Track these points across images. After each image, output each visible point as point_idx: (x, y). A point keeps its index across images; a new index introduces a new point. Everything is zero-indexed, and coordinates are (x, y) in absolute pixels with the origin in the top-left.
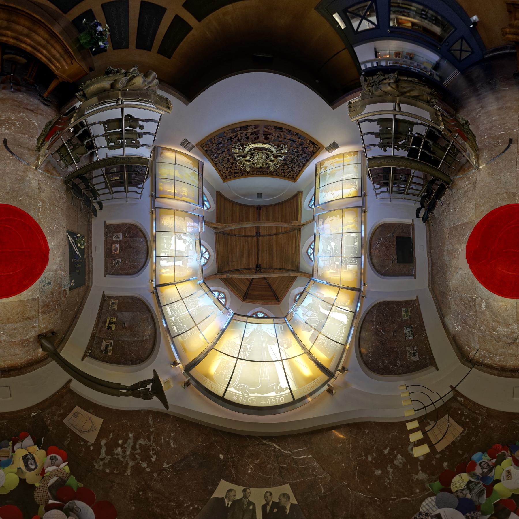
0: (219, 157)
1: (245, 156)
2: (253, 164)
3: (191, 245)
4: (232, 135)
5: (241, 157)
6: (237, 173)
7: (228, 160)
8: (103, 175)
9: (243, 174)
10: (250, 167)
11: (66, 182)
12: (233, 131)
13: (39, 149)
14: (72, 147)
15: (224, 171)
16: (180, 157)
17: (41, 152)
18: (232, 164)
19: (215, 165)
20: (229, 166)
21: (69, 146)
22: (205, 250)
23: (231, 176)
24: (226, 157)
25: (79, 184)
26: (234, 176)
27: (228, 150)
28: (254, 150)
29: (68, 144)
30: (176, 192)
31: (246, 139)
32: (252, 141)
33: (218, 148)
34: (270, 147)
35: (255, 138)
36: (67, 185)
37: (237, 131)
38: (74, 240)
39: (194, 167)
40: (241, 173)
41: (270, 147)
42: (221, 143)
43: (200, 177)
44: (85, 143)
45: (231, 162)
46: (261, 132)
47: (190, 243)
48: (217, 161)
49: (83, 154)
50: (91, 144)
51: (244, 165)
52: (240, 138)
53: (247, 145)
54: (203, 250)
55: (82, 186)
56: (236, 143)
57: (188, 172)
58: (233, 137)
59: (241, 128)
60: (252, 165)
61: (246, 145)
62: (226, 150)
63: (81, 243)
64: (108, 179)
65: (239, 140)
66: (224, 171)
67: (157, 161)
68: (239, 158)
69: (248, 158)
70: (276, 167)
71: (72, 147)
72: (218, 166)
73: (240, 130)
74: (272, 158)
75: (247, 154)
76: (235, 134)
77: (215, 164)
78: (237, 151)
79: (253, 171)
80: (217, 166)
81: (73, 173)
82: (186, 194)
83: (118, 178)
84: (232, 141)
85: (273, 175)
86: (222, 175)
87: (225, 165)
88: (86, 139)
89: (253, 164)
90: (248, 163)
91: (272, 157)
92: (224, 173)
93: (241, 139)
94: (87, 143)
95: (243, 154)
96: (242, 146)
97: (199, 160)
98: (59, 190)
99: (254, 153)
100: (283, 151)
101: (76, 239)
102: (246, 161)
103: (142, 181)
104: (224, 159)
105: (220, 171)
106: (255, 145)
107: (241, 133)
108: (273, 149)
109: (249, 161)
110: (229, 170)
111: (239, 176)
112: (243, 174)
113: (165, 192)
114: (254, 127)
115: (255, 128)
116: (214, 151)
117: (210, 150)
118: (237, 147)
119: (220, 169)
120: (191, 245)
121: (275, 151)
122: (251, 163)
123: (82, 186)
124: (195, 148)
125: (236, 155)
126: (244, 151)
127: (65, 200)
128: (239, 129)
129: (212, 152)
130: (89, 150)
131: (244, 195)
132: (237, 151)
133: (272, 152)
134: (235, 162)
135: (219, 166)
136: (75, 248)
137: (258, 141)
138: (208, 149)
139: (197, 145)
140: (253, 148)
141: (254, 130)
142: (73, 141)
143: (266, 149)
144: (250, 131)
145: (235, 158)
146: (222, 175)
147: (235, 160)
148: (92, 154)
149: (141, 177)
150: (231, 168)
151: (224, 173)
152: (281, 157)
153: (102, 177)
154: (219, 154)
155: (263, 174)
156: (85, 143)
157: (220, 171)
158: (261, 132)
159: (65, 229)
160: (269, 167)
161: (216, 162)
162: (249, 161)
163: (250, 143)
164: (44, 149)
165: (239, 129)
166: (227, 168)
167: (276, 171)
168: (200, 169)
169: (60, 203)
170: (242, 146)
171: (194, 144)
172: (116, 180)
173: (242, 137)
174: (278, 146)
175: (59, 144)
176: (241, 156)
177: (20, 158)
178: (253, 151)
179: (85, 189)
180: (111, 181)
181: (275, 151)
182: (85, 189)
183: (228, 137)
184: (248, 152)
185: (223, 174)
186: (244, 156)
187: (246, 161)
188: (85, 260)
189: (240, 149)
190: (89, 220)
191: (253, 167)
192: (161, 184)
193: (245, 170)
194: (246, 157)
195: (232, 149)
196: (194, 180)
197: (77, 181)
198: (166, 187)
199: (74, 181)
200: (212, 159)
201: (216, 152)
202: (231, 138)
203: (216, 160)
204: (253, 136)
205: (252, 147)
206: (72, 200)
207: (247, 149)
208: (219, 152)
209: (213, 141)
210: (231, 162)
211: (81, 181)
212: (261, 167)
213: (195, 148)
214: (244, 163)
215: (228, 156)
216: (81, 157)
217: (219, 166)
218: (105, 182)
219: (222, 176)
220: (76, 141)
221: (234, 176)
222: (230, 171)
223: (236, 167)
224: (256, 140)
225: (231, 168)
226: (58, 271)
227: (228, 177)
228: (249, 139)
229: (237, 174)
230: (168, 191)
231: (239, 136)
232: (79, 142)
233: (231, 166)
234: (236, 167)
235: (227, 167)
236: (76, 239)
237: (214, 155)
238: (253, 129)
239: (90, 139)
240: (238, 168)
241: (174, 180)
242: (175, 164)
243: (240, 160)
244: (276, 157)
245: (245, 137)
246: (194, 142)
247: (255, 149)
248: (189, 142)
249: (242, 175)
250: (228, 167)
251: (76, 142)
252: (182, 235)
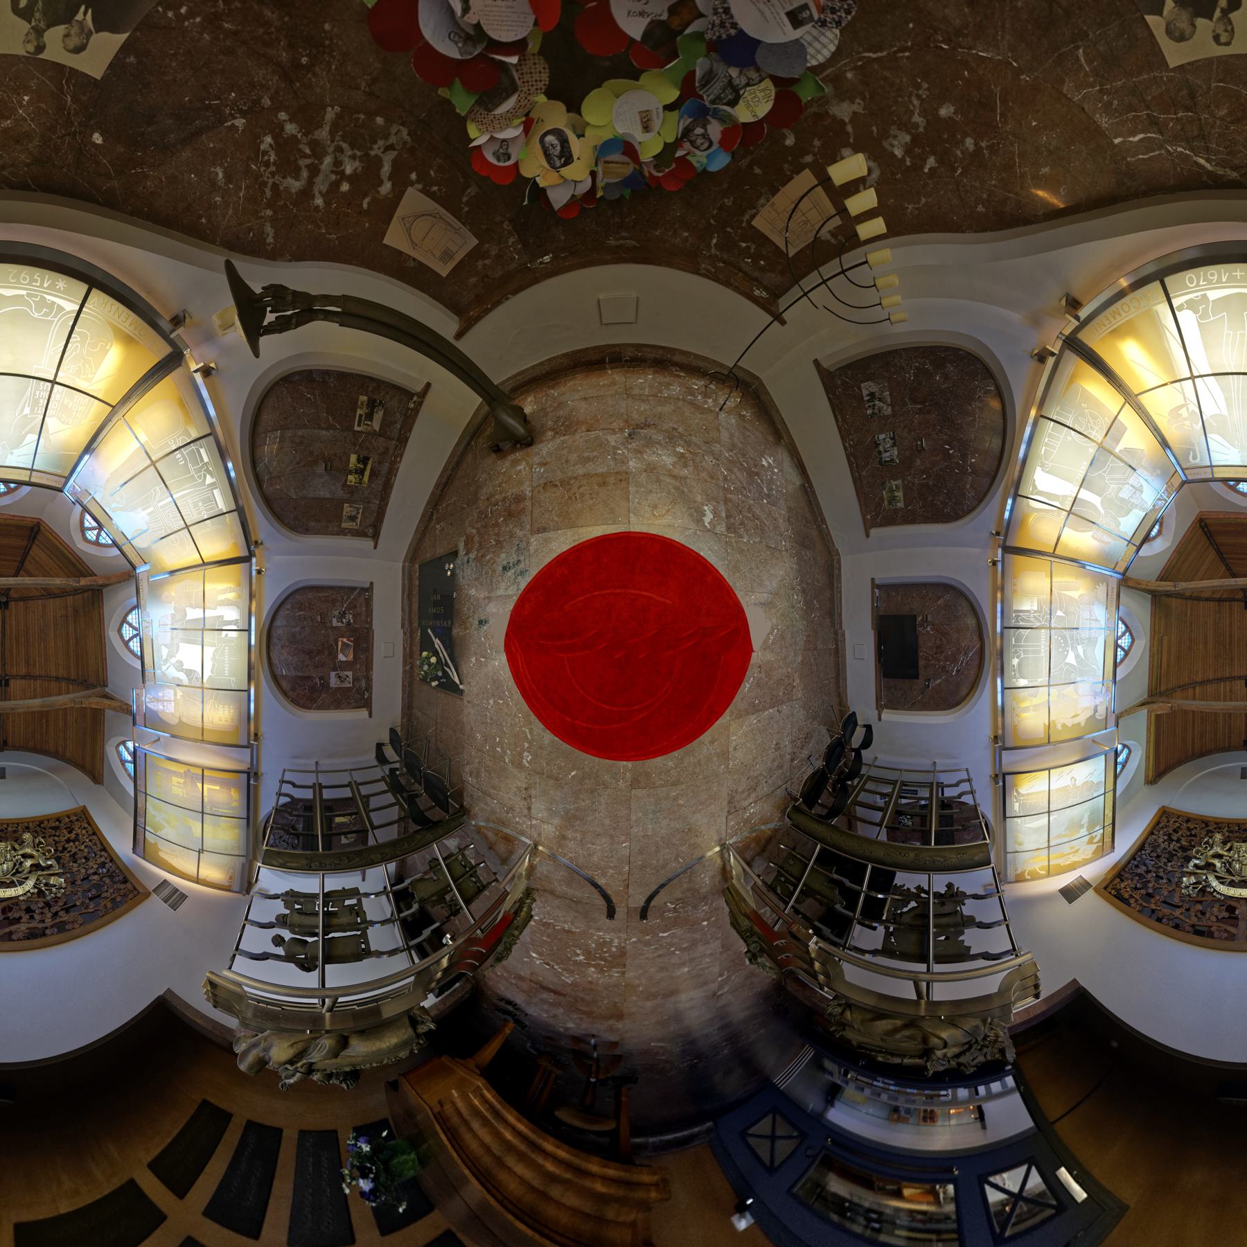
0: (96, 866)
1: (34, 868)
2: (15, 850)
3: (164, 658)
4: (64, 917)
5: (43, 864)
6: (52, 828)
7: (74, 858)
8: (374, 828)
9: (39, 826)
10: (22, 843)
11: (463, 812)
12: (61, 927)
13: (528, 893)
14: (448, 898)
15: (84, 832)
16: (189, 866)
17: (522, 885)
18: (64, 849)
19: (105, 847)
20: (71, 844)
21: (454, 900)
22: (131, 644)
23: (67, 820)
24: (79, 865)
25: (432, 808)
26: (60, 822)
27: (73, 883)
28: (13, 882)
29: (456, 903)
30: (200, 785)
31: (33, 907)
32: (17, 904)
33: (98, 886)
35: (10, 909)
36: (462, 806)
37: (52, 926)
38: (445, 672)
39: (156, 843)
40: (45, 828)
42: (91, 899)
43: (140, 820)
44: (415, 907)
45: (68, 855)
47: (166, 661)
48: (101, 856)
49: (422, 879)
50: (402, 904)
51: (36, 846)
52: (46, 910)
53: (29, 894)
54: (135, 645)
55: (424, 801)
56: (56, 899)
57: (169, 832)
58: (62, 913)
59: (44, 935)
60: (17, 846)
61: (32, 894)
62: (79, 882)
63: (430, 665)
64: (361, 817)
65: (48, 905)
66: (84, 832)
67: (243, 860)
68: (49, 863)
69: (28, 863)
71: (448, 898)
72: (99, 845)
73: (46, 928)
75: (30, 872)
76: (58, 920)
77: (104, 849)
78: (52, 881)
79: (15, 832)
80: (102, 844)
81: (446, 833)
82: (175, 779)
83: (338, 820)
84: (65, 904)
86: (89, 824)
87: (82, 847)
88: (413, 915)
89: (15, 850)
90: (28, 851)
92: (85, 828)
93: (42, 908)
94: (410, 907)
95: (40, 873)
96: (41, 893)
97: (144, 859)
98: (480, 794)
99: (14, 875)
101: (440, 674)
102: (31, 857)
103: (281, 811)
104: (84, 861)
105: (94, 834)
107: (44, 922)
109: (25, 856)
110: (73, 836)
111: (48, 820)
112: (39, 826)
113: (225, 784)
114: (14, 937)
115: (11, 933)
116: (107, 880)
117: (116, 883)
118: (54, 889)
119: (95, 837)
120: (164, 658)
122: (21, 852)
123: (424, 801)
124: (151, 888)
125: (57, 869)
126: (38, 879)
127: (467, 769)
128: (48, 932)
129: (111, 877)
130: (406, 889)
131: (37, 774)
132: (52, 881)
134: (58, 854)
135: (95, 844)
136: (444, 654)
137: (4, 904)
138: (122, 886)
139: (148, 895)
140: (16, 886)
141: (13, 928)
142: (445, 913)
144: (23, 927)
145: (58, 863)
146: (89, 824)
147: (58, 859)
148: (399, 878)
149: (281, 821)
150: (68, 841)
151: (85, 828)
153: (376, 823)
154: (95, 873)
156: (415, 907)
157: (94, 834)
159: (466, 698)
161: (103, 853)
162: (25, 856)
163: (21, 898)
164: (516, 894)
165: (48, 932)
168: (140, 837)
169: (479, 763)
170: (41, 893)
171: (154, 896)
172: (343, 815)
173: (42, 913)
175: (480, 905)
176: (43, 869)
177: (575, 874)
178: (15, 879)
179: (417, 796)
180: (356, 814)
182: (417, 796)
183: (73, 914)
184: (27, 878)
185: (86, 825)
186: (36, 867)
187: (31, 857)
188: (420, 624)
189: (46, 885)
190: (409, 720)
191: (16, 841)
192: (235, 804)
193: (35, 834)
194: (31, 865)
195: (64, 885)
196: (155, 813)
197: (436, 814)
198: (223, 796)
199: (444, 814)
200: (112, 860)
201: (101, 878)
202: (67, 910)
203: (103, 859)
204: (16, 915)
205: (19, 888)
206: (450, 767)
207: (29, 885)
208: (96, 877)
209: (109, 905)
210: (68, 855)
211: (426, 813)
213: (151, 888)
214: (38, 851)
215: (75, 869)
216: (426, 873)
217: (95, 844)
218: (368, 812)
219: (90, 822)
220: (438, 911)
221: (60, 822)
222: (70, 832)
223: (56, 843)
225: (68, 841)
226: (484, 599)
227: (75, 818)
228: (24, 907)
229: (53, 825)
230: (218, 788)
231: (49, 915)
232: (429, 908)
233: (67, 846)
234: (56, 843)
235: (77, 843)
236: (440, 674)
237: (108, 870)
238: (16, 931)
239: (402, 915)
240: (51, 839)
241: (203, 813)
242: (201, 851)
243: (47, 859)
245: (34, 912)
246: (155, 902)
247: (12, 885)
248: (166, 902)
249: (42, 822)
250: (74, 841)
251: (438, 908)
252: (185, 681)
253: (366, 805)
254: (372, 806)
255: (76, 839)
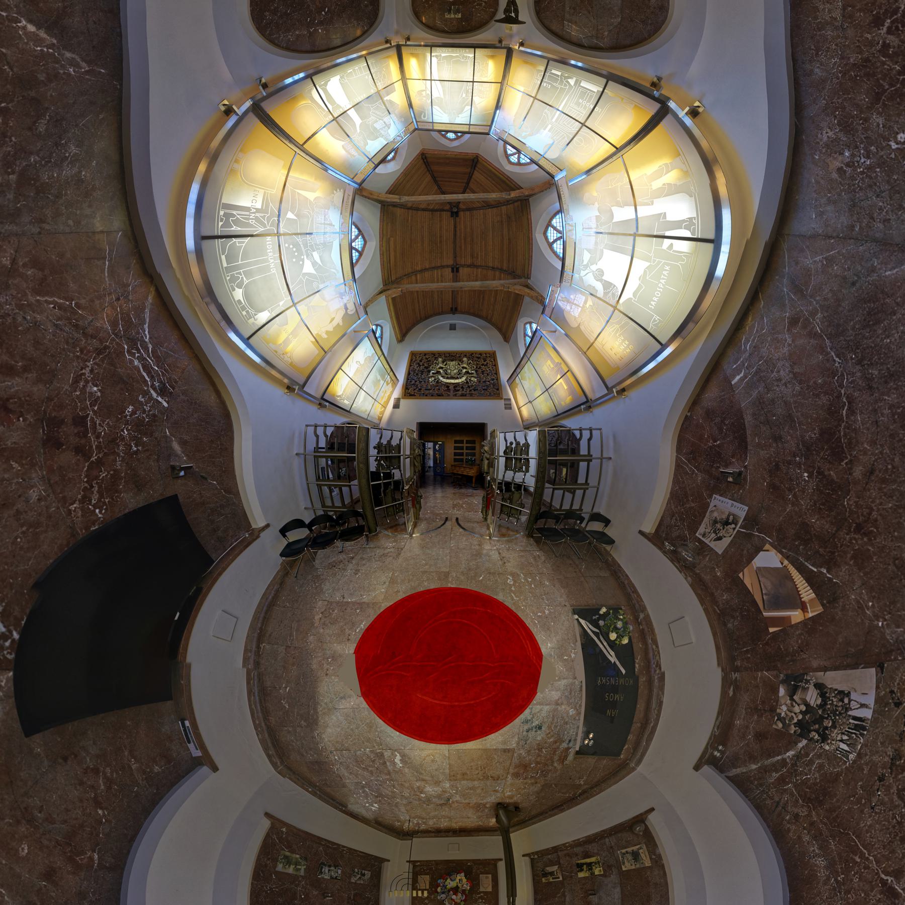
2: (459, 365)
18: (480, 368)
23: (485, 355)
34: (445, 380)
41: (445, 380)
46: (452, 392)
51: (469, 364)
56: (472, 386)
69: (464, 371)
70: (436, 363)
74: (441, 371)
83: (564, 470)
85: (438, 354)
89: (459, 365)
90: (465, 366)
91: (442, 371)
100: (433, 379)
102: (466, 368)
106: (457, 381)
108: (441, 379)
109: (463, 368)
110: (485, 363)
121: (440, 377)
125: (475, 375)
132: (472, 379)
133: (442, 376)
143: (448, 378)
144: (460, 393)
147: (476, 371)
150: (483, 365)
152: (433, 373)
155: (449, 354)
157: (495, 365)
158: (452, 392)
160: (443, 362)
166: (486, 365)
167: (436, 358)
174: (437, 382)
176: (470, 374)
180: (566, 482)
181: (440, 377)
186: (467, 373)
187: (466, 368)
207: (464, 379)
212: (452, 361)
224: (456, 385)
244: (438, 373)
247: (457, 378)
253: (569, 490)
254: (566, 493)
255: (486, 365)
